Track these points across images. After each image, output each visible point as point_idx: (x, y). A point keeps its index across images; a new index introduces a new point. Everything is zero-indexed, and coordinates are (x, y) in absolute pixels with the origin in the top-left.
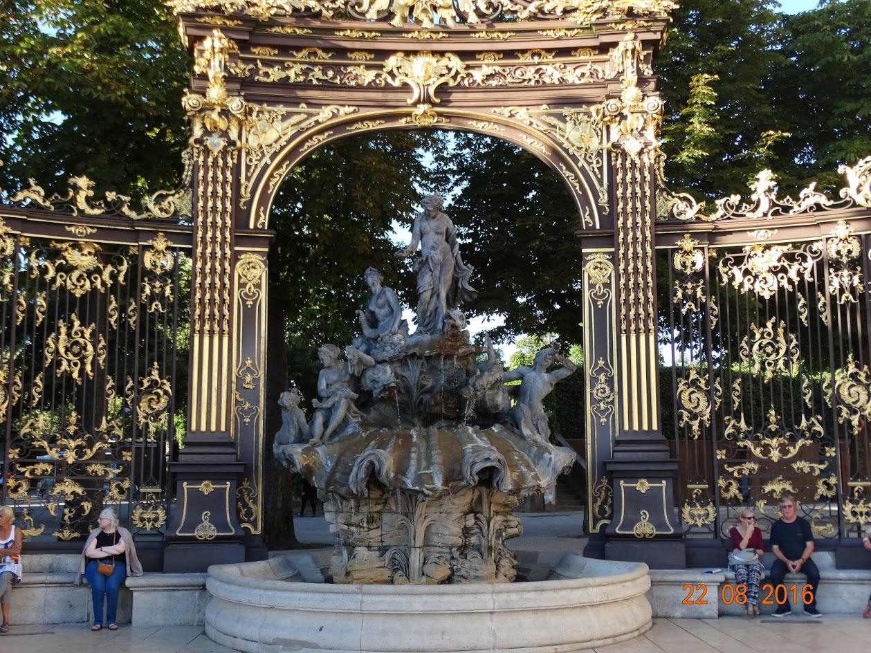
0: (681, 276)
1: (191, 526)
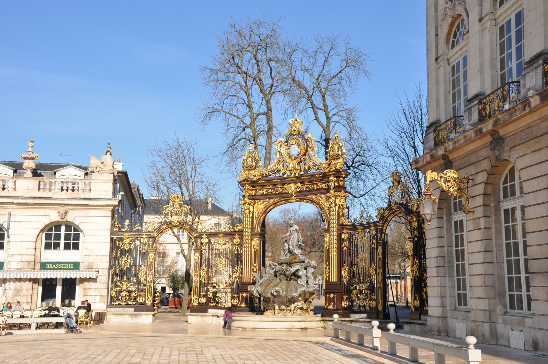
0: (343, 240)
1: (240, 304)
